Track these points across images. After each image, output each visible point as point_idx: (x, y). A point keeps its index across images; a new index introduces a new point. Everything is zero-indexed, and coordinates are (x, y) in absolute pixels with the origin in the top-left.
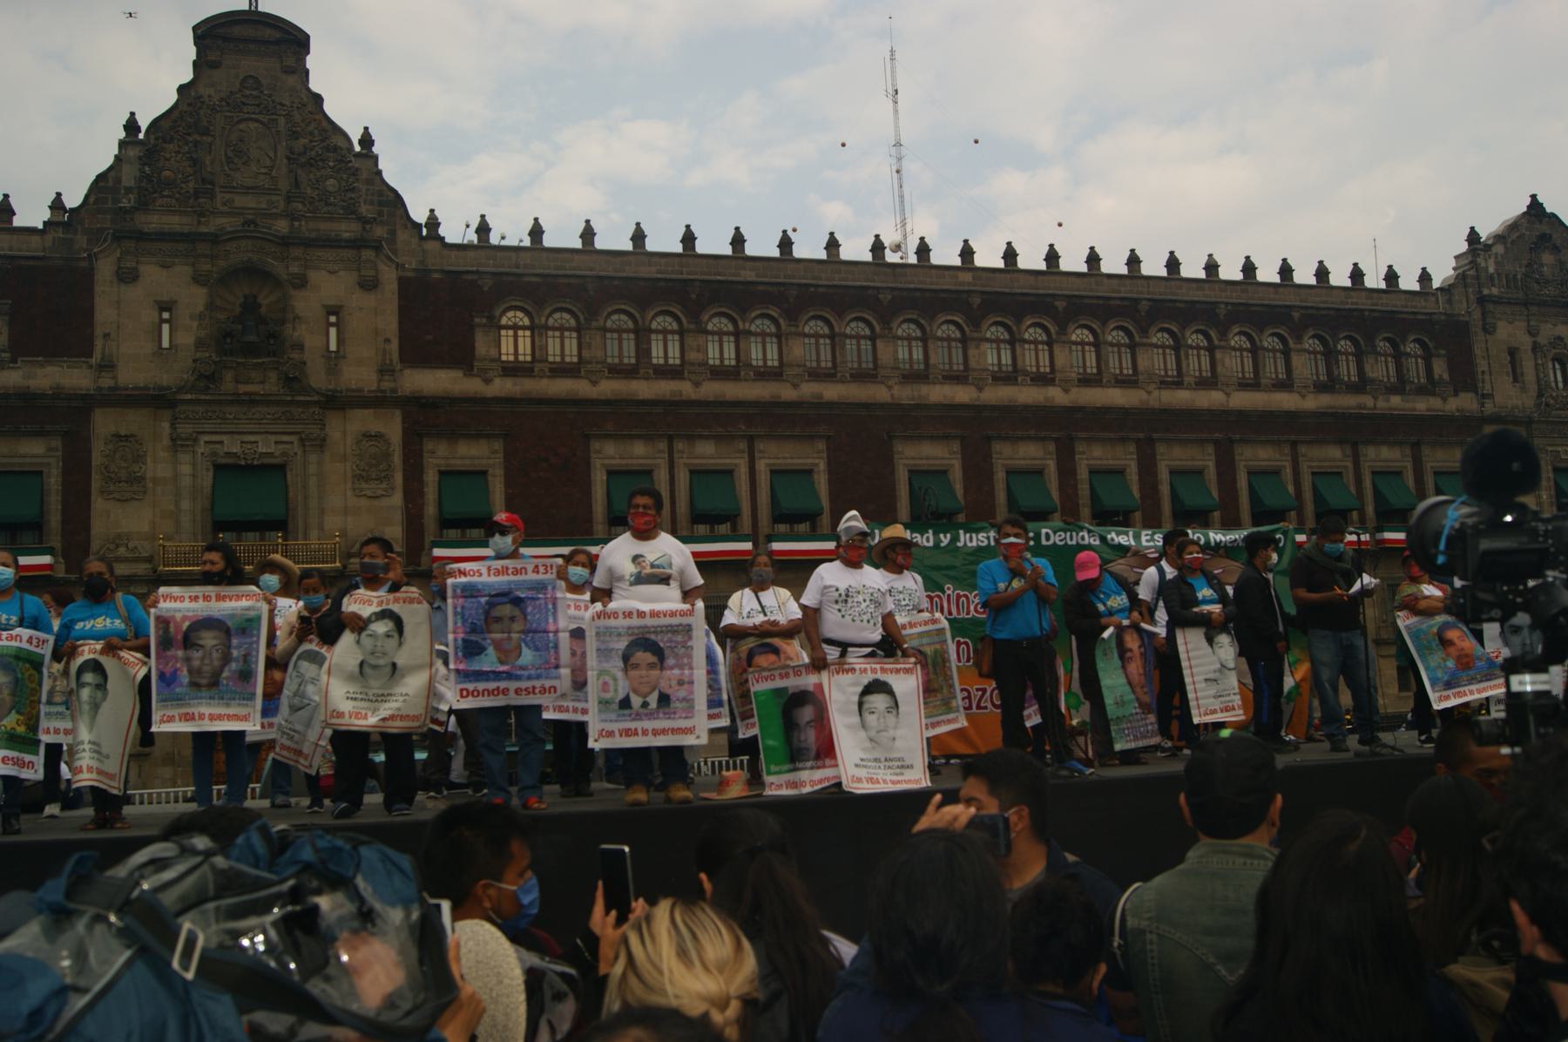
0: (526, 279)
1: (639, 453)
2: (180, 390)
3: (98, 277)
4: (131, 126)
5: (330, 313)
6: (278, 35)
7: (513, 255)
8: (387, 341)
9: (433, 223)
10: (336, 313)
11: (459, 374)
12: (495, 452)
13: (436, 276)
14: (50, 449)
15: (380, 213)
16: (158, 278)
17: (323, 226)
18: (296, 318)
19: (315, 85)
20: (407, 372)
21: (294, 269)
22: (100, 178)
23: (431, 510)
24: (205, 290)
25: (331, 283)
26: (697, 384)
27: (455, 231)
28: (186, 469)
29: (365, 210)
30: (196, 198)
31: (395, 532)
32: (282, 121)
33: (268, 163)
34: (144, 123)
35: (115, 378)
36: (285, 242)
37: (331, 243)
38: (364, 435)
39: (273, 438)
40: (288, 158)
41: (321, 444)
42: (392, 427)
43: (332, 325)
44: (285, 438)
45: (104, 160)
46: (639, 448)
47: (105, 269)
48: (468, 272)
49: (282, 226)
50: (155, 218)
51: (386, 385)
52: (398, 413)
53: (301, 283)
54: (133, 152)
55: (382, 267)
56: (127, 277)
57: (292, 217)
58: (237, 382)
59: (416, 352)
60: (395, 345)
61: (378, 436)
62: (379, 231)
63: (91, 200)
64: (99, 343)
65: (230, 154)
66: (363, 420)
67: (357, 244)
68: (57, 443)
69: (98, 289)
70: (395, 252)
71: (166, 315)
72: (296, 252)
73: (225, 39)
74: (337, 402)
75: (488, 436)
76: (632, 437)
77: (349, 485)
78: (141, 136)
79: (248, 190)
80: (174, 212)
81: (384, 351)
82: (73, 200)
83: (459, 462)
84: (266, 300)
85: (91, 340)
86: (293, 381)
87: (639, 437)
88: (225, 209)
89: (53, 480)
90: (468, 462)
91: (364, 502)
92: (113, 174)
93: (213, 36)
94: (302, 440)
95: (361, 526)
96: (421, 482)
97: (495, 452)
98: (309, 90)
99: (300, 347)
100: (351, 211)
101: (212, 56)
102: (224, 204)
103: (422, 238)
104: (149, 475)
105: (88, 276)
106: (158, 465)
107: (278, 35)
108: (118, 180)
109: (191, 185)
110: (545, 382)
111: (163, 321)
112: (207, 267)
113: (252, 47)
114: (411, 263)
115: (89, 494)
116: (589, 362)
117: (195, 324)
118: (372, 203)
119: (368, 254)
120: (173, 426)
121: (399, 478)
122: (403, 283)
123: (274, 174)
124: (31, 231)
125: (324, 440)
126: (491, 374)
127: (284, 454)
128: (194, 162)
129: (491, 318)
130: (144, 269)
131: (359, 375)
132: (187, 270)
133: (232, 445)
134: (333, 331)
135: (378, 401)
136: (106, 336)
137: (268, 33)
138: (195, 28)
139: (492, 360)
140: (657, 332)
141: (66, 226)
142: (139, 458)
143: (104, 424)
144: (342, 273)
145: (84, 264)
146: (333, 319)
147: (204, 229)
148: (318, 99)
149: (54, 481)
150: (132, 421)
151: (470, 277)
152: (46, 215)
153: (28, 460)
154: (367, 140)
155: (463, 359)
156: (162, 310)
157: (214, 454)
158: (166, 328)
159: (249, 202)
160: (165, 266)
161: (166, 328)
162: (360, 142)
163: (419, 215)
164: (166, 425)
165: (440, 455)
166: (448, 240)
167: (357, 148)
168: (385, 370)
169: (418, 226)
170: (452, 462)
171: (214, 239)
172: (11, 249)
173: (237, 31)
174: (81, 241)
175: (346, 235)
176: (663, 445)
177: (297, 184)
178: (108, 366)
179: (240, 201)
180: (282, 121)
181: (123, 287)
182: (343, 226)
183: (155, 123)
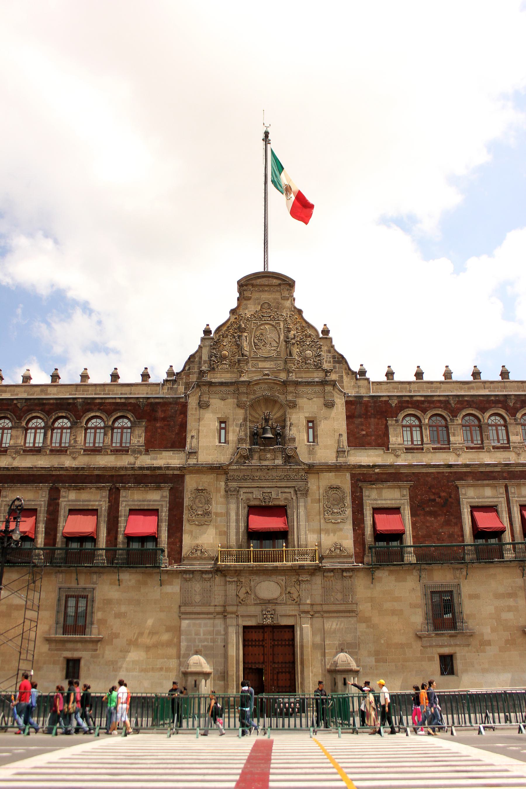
0: (415, 399)
1: (488, 494)
2: (230, 464)
3: (189, 407)
4: (207, 332)
5: (309, 422)
6: (279, 282)
7: (408, 386)
8: (340, 435)
9: (363, 373)
10: (312, 422)
11: (381, 452)
12: (404, 496)
13: (366, 399)
14: (162, 497)
15: (334, 367)
16: (221, 406)
17: (303, 375)
18: (291, 424)
19: (298, 305)
20: (352, 452)
21: (290, 398)
22: (192, 357)
23: (368, 531)
24: (242, 411)
25: (308, 406)
26: (519, 454)
27: (376, 374)
28: (233, 507)
29: (326, 366)
30: (239, 364)
31: (348, 543)
32: (282, 324)
33: (276, 345)
34: (213, 330)
35: (197, 458)
36: (285, 384)
37: (309, 384)
38: (331, 488)
39: (280, 490)
40: (286, 342)
41: (306, 493)
42: (345, 482)
43: (311, 428)
44: (287, 490)
45: (193, 349)
46: (488, 492)
47: (192, 402)
48: (383, 396)
49: (283, 376)
50: (218, 375)
51: (341, 460)
52: (348, 475)
53: (293, 405)
54: (208, 343)
55: (336, 395)
56: (203, 405)
57: (289, 372)
58: (260, 459)
59: (357, 440)
60: (345, 438)
61: (338, 488)
62: (333, 377)
63: (187, 368)
64: (188, 440)
65: (256, 341)
66: (329, 479)
67: (323, 383)
68: (166, 493)
69: (189, 413)
70: (343, 387)
71: (223, 425)
72: (291, 389)
73: (253, 285)
74: (312, 469)
75: (400, 487)
76: (484, 486)
77: (322, 516)
78: (212, 335)
79: (266, 359)
80: (228, 372)
81: (339, 442)
82: (177, 369)
83: (384, 502)
84: (275, 414)
85: (185, 438)
86: (290, 458)
87: (488, 485)
88: (254, 369)
89: (164, 514)
90: (389, 502)
91: (330, 526)
92: (198, 354)
93: (248, 285)
94: (295, 491)
95: (328, 541)
96: (362, 514)
97: (404, 496)
98: (295, 308)
99: (294, 440)
100: (318, 367)
101: (247, 294)
102: (252, 367)
103: (357, 379)
104: (214, 510)
105: (185, 406)
106: (217, 505)
107: (279, 282)
108: (201, 358)
109: (237, 357)
110: (430, 455)
111: (221, 428)
112: (245, 399)
113: (266, 289)
114: (352, 393)
115: (182, 522)
116: (456, 444)
117: (238, 429)
118: (330, 362)
119: (329, 388)
120: (227, 485)
121: (349, 512)
122: (348, 403)
123: (278, 350)
124: (158, 385)
125: (308, 491)
126: (399, 453)
127: (286, 499)
128: (238, 345)
129: (397, 421)
130: (212, 401)
131: (326, 454)
132: (236, 401)
133: (257, 494)
134: (311, 431)
135: (337, 468)
136: (192, 437)
137: (276, 282)
138: (238, 282)
139: (399, 444)
140: (492, 425)
141: (175, 381)
142: (208, 502)
143: (191, 483)
144: (315, 399)
145: (183, 400)
146: (311, 425)
147: (242, 379)
148: (300, 312)
149: (164, 514)
150: (205, 481)
151: (384, 399)
152: (165, 377)
153: (151, 503)
154: (326, 332)
155: (382, 442)
156: (221, 422)
157: (248, 499)
158: (223, 432)
159: (267, 365)
160: (223, 399)
161: (223, 432)
162: (323, 332)
163: (355, 368)
164: (223, 484)
165: (373, 497)
166: (372, 380)
167: (321, 335)
168: (340, 452)
169: (354, 373)
170: (379, 502)
171: (248, 383)
172: (147, 394)
173: (258, 281)
174: (181, 389)
175: (317, 380)
176: (502, 490)
177: (291, 355)
178: (193, 453)
179: (261, 365)
180: (282, 324)
181: (202, 411)
182: (315, 375)
183: (219, 329)
